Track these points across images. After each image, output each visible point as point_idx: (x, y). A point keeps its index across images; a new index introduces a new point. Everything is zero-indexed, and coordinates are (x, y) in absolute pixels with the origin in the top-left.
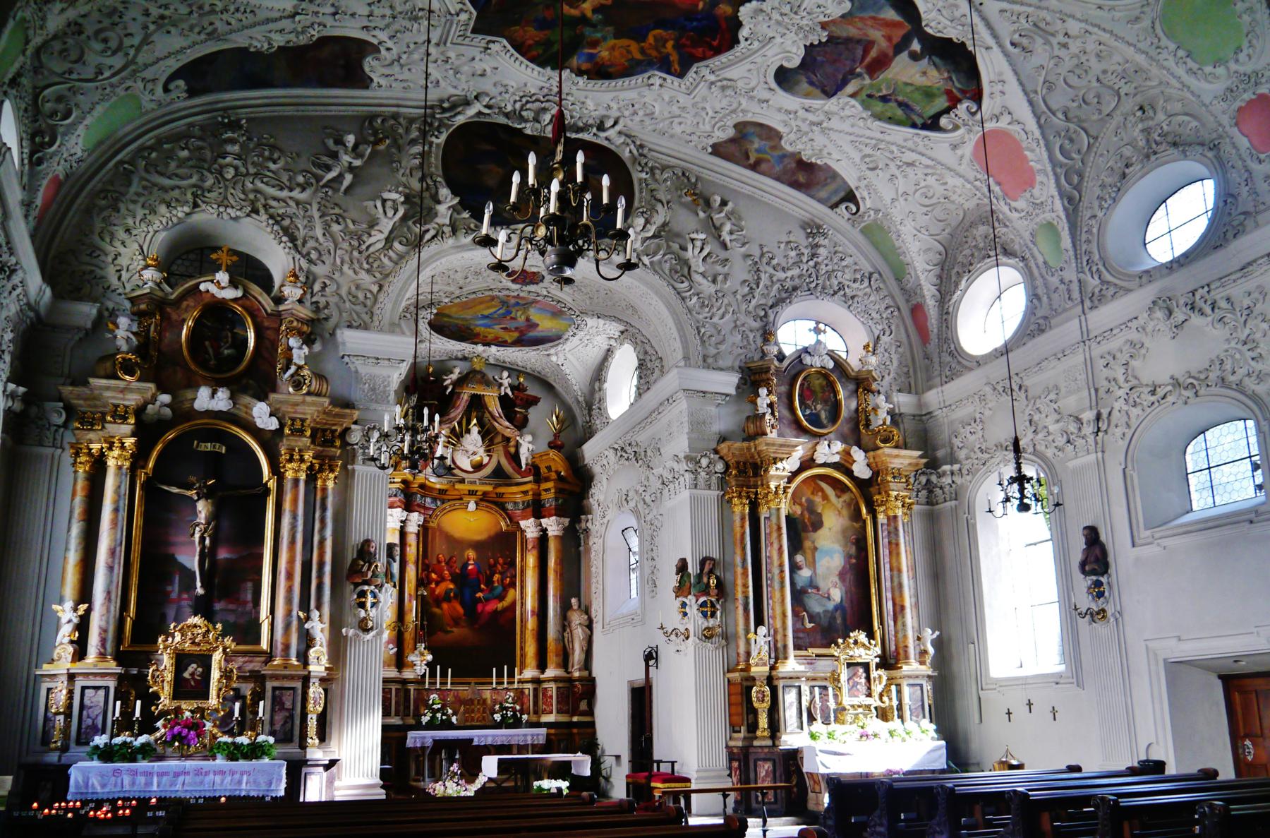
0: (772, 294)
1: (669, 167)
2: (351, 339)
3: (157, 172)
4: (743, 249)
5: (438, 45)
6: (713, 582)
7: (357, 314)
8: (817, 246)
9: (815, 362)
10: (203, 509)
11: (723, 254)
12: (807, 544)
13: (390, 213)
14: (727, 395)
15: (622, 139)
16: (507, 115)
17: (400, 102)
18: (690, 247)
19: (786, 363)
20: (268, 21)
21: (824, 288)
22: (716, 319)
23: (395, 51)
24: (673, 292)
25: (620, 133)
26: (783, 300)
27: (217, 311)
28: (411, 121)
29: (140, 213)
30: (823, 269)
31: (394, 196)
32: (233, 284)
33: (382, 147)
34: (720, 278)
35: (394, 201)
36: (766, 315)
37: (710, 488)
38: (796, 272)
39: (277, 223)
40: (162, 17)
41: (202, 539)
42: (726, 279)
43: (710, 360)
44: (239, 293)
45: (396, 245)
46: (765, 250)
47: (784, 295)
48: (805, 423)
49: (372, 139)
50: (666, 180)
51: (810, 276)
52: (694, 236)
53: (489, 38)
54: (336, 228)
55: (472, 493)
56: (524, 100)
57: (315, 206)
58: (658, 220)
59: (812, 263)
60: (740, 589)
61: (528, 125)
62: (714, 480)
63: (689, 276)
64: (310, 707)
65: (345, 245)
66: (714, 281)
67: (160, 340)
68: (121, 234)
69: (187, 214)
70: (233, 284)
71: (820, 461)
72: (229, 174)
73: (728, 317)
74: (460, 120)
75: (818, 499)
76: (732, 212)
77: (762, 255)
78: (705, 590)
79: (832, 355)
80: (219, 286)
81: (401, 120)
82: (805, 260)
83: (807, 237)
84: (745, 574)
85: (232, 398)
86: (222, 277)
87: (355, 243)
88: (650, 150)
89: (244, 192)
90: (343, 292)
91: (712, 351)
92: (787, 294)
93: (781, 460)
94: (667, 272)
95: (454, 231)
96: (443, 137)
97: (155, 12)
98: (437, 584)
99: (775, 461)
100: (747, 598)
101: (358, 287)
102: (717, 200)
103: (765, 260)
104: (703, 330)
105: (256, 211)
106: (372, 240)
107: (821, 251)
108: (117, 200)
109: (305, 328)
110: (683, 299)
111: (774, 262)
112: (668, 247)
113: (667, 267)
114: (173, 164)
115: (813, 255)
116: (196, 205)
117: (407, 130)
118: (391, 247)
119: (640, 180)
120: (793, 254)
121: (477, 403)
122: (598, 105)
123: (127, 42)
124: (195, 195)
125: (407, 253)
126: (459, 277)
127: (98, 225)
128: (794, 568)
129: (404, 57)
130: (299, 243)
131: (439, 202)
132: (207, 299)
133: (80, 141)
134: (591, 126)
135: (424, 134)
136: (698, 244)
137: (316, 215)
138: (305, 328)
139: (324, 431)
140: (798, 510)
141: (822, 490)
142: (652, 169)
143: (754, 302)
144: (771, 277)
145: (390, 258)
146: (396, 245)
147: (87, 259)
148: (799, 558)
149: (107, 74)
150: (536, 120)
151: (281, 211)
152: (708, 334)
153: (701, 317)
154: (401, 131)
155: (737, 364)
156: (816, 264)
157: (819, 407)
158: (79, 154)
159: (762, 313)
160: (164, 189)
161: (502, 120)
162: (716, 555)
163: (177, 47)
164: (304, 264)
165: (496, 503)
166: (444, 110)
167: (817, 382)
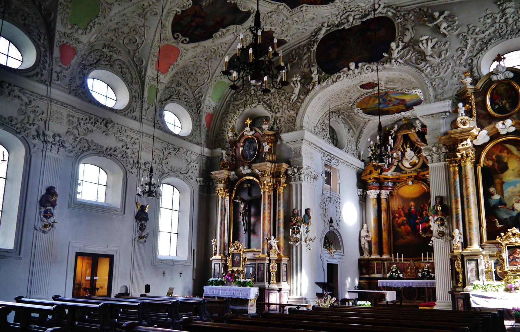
0: (476, 48)
1: (412, 10)
2: (286, 137)
3: (237, 101)
4: (457, 32)
5: (287, 19)
6: (439, 208)
7: (290, 127)
8: (505, 9)
9: (501, 77)
10: (242, 206)
11: (444, 40)
12: (497, 181)
13: (296, 85)
14: (446, 112)
15: (385, 10)
16: (337, 26)
17: (300, 41)
18: (421, 45)
19: (480, 85)
20: (232, 43)
21: (512, 30)
22: (441, 75)
23: (278, 29)
24: (415, 70)
25: (384, 7)
26: (482, 49)
27: (250, 140)
28: (304, 46)
29: (232, 115)
30: (510, 21)
31: (295, 79)
32: (251, 129)
33: (295, 61)
34: (443, 53)
35: (296, 81)
36: (472, 62)
37: (440, 161)
38: (493, 29)
39: (266, 103)
40: (206, 59)
41: (243, 216)
42: (447, 52)
43: (438, 97)
44: (254, 132)
45: (302, 97)
46: (470, 27)
47: (483, 46)
48: (497, 115)
49: (292, 60)
50: (411, 17)
51: (501, 28)
52: (421, 39)
53: (299, 7)
54: (283, 98)
55: (410, 177)
56: (339, 16)
57: (276, 93)
58: (407, 39)
59: (502, 21)
60: (454, 210)
61: (345, 25)
62: (442, 157)
63: (425, 60)
64: (271, 270)
65: (285, 103)
66: (439, 57)
67: (236, 154)
68: (229, 124)
69: (243, 111)
70: (251, 129)
71: (503, 132)
72: (253, 92)
73: (449, 71)
74: (320, 37)
75: (504, 154)
76: (449, 16)
77: (469, 30)
78: (436, 213)
79: (511, 69)
80: (248, 133)
81: (301, 48)
82: (497, 21)
83: (499, 8)
84: (457, 202)
85: (250, 167)
86: (248, 129)
87: (288, 101)
88: (402, 7)
89: (257, 97)
90: (286, 120)
91: (440, 91)
92: (485, 45)
93: (466, 139)
94: (414, 61)
95: (319, 83)
96: (315, 47)
97: (203, 59)
98: (399, 219)
99: (462, 141)
100: (457, 214)
101: (290, 117)
102: (437, 14)
103: (470, 32)
104: (434, 83)
105: (259, 102)
106: (292, 98)
107: (507, 11)
108: (227, 113)
109: (272, 137)
110: (422, 71)
111: (478, 30)
112: (414, 49)
113: (413, 59)
114: (239, 96)
115: (503, 16)
116: (245, 107)
117: (303, 51)
118: (300, 98)
119: (398, 24)
120: (489, 21)
121: (406, 138)
122: (364, 3)
123: (205, 70)
124: (245, 104)
125: (305, 98)
126: (342, 95)
127: (224, 123)
128: (488, 195)
129: (283, 28)
130: (272, 108)
131: (312, 73)
132: (246, 137)
133: (211, 101)
134: (371, 11)
135: (309, 49)
136: (424, 42)
137: (277, 95)
138: (272, 137)
139: (277, 172)
140: (490, 163)
141: (507, 149)
142: (404, 16)
143: (464, 57)
144: (475, 39)
145: (299, 102)
146: (302, 97)
147: (222, 134)
148: (492, 190)
149: (206, 81)
150: (348, 21)
151: (267, 99)
152: (438, 83)
153: (433, 76)
154: (301, 52)
155: (455, 93)
156: (506, 19)
157: (504, 102)
158: (214, 105)
159: (470, 61)
160: (238, 105)
161: (336, 29)
162: (444, 194)
163: (217, 64)
164: (274, 114)
165: (421, 180)
166: (314, 36)
167: (502, 88)
